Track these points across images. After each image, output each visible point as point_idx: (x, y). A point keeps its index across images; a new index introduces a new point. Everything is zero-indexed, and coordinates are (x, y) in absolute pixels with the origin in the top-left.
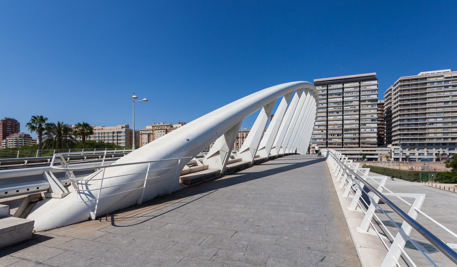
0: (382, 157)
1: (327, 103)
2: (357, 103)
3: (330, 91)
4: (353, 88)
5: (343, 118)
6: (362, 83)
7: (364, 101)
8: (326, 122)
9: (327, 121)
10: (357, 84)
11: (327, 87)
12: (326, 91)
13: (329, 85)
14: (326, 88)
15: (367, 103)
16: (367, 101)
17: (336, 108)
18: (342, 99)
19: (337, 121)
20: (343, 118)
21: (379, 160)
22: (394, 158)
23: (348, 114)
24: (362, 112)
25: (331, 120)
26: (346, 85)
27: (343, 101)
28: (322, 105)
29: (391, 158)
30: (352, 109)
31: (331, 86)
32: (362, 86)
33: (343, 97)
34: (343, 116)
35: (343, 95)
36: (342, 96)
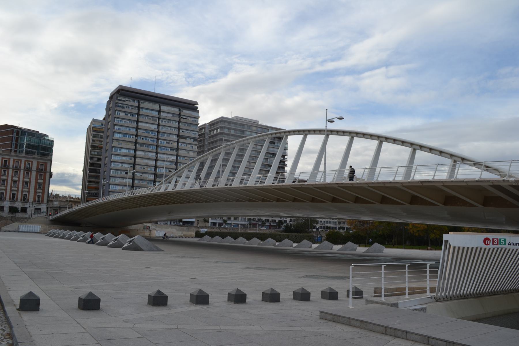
0: (198, 220)
1: (137, 129)
2: (175, 138)
3: (142, 111)
4: (172, 115)
5: (157, 157)
6: (183, 111)
7: (184, 138)
8: (133, 158)
9: (135, 157)
10: (176, 110)
11: (139, 103)
12: (136, 109)
13: (141, 101)
14: (136, 104)
15: (188, 141)
16: (188, 139)
17: (148, 140)
18: (156, 127)
19: (148, 161)
20: (157, 157)
21: (195, 224)
22: (211, 223)
23: (163, 152)
24: (181, 152)
25: (140, 157)
26: (164, 108)
27: (158, 130)
28: (130, 130)
29: (208, 222)
30: (168, 145)
31: (144, 103)
32: (183, 115)
33: (159, 125)
34: (157, 153)
35: (158, 122)
36: (158, 124)
